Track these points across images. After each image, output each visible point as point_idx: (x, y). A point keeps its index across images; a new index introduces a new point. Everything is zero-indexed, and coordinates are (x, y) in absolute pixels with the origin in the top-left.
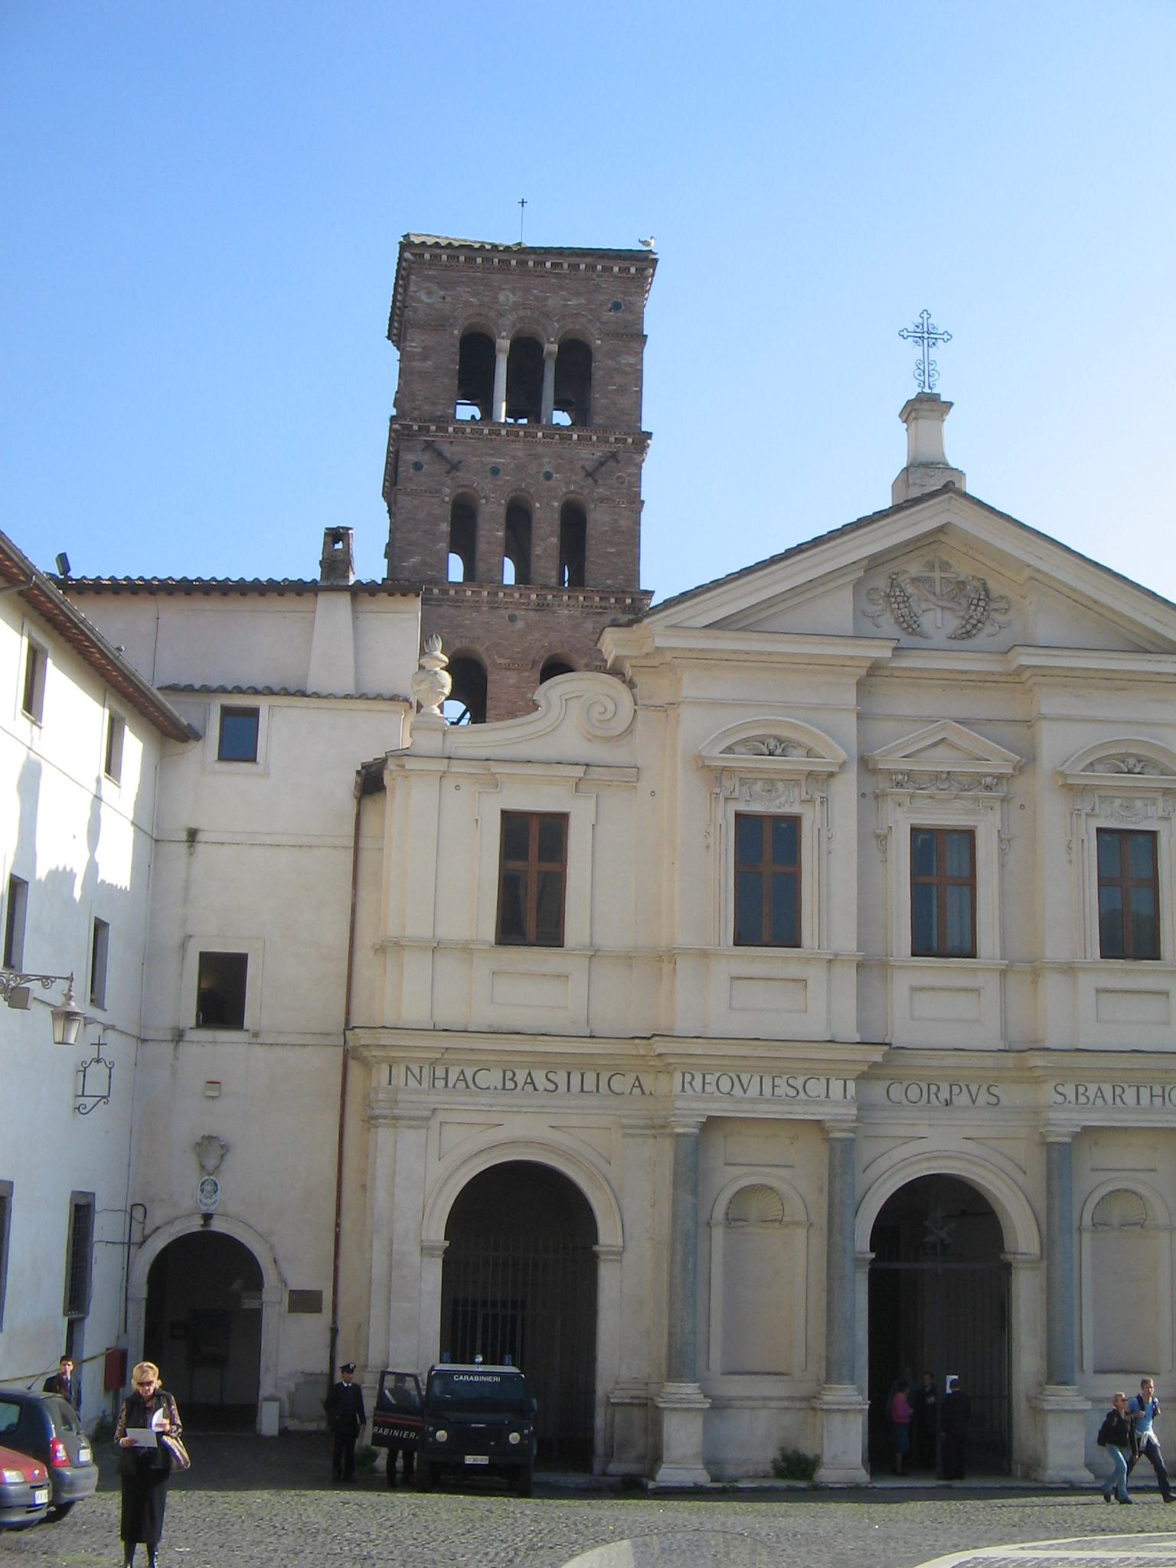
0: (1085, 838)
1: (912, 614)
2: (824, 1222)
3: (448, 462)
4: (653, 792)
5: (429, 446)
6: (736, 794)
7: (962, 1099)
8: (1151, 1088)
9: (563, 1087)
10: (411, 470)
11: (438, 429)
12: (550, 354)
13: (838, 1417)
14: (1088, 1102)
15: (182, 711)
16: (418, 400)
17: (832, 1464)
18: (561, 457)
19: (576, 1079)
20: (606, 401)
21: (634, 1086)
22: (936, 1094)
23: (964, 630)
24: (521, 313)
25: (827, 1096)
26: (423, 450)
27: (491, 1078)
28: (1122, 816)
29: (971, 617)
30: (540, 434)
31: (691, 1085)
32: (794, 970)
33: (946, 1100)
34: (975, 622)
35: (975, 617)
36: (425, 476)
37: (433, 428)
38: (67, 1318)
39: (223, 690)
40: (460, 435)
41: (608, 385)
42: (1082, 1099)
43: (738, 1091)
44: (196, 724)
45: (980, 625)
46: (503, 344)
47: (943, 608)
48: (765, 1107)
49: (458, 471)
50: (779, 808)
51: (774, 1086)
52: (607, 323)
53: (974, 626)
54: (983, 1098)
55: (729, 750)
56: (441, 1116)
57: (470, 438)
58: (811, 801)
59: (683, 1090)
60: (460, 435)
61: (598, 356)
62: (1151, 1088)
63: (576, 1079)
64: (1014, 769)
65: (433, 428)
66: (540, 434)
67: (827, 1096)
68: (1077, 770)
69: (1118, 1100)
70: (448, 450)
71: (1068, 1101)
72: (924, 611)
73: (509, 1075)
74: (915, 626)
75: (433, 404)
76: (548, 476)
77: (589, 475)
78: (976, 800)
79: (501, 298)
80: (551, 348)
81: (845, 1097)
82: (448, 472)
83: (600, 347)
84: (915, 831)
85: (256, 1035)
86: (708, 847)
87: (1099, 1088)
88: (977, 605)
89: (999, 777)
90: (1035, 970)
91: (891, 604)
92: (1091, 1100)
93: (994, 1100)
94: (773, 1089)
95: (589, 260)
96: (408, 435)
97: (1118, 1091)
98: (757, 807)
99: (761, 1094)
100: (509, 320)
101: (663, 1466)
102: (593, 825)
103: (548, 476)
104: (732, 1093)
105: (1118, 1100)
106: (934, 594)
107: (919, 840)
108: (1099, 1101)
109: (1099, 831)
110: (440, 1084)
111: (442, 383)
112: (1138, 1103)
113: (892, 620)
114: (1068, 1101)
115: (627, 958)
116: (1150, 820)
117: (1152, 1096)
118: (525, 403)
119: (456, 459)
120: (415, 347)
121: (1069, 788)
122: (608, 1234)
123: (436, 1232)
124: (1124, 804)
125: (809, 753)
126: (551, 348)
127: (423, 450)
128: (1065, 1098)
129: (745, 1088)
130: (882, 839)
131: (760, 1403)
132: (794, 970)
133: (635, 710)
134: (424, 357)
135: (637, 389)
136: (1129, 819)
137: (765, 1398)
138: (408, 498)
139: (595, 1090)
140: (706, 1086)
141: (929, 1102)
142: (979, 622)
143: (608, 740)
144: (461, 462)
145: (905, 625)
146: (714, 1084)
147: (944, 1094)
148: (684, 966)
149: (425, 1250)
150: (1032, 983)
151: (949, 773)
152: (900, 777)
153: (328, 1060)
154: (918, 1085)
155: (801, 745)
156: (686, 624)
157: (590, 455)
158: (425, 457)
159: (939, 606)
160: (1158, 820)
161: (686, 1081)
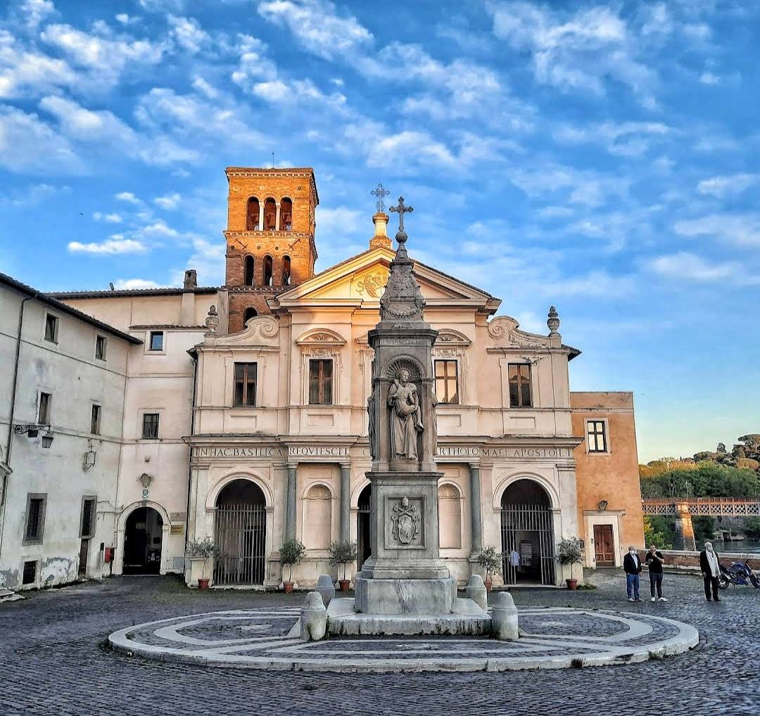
2: (338, 496)
9: (254, 454)
15: (133, 334)
18: (282, 242)
19: (259, 451)
27: (230, 452)
32: (328, 412)
38: (81, 539)
39: (152, 327)
43: (309, 453)
44: (143, 340)
46: (262, 205)
56: (212, 465)
58: (335, 355)
63: (259, 451)
73: (236, 450)
76: (277, 248)
77: (291, 247)
79: (261, 188)
80: (278, 204)
85: (161, 440)
95: (289, 173)
97: (442, 450)
98: (317, 358)
100: (262, 196)
103: (277, 248)
110: (213, 454)
118: (269, 226)
122: (269, 503)
123: (211, 503)
126: (278, 204)
130: (362, 366)
132: (328, 412)
134: (234, 210)
148: (293, 413)
149: (208, 511)
153: (181, 448)
156: (291, 298)
157: (291, 240)
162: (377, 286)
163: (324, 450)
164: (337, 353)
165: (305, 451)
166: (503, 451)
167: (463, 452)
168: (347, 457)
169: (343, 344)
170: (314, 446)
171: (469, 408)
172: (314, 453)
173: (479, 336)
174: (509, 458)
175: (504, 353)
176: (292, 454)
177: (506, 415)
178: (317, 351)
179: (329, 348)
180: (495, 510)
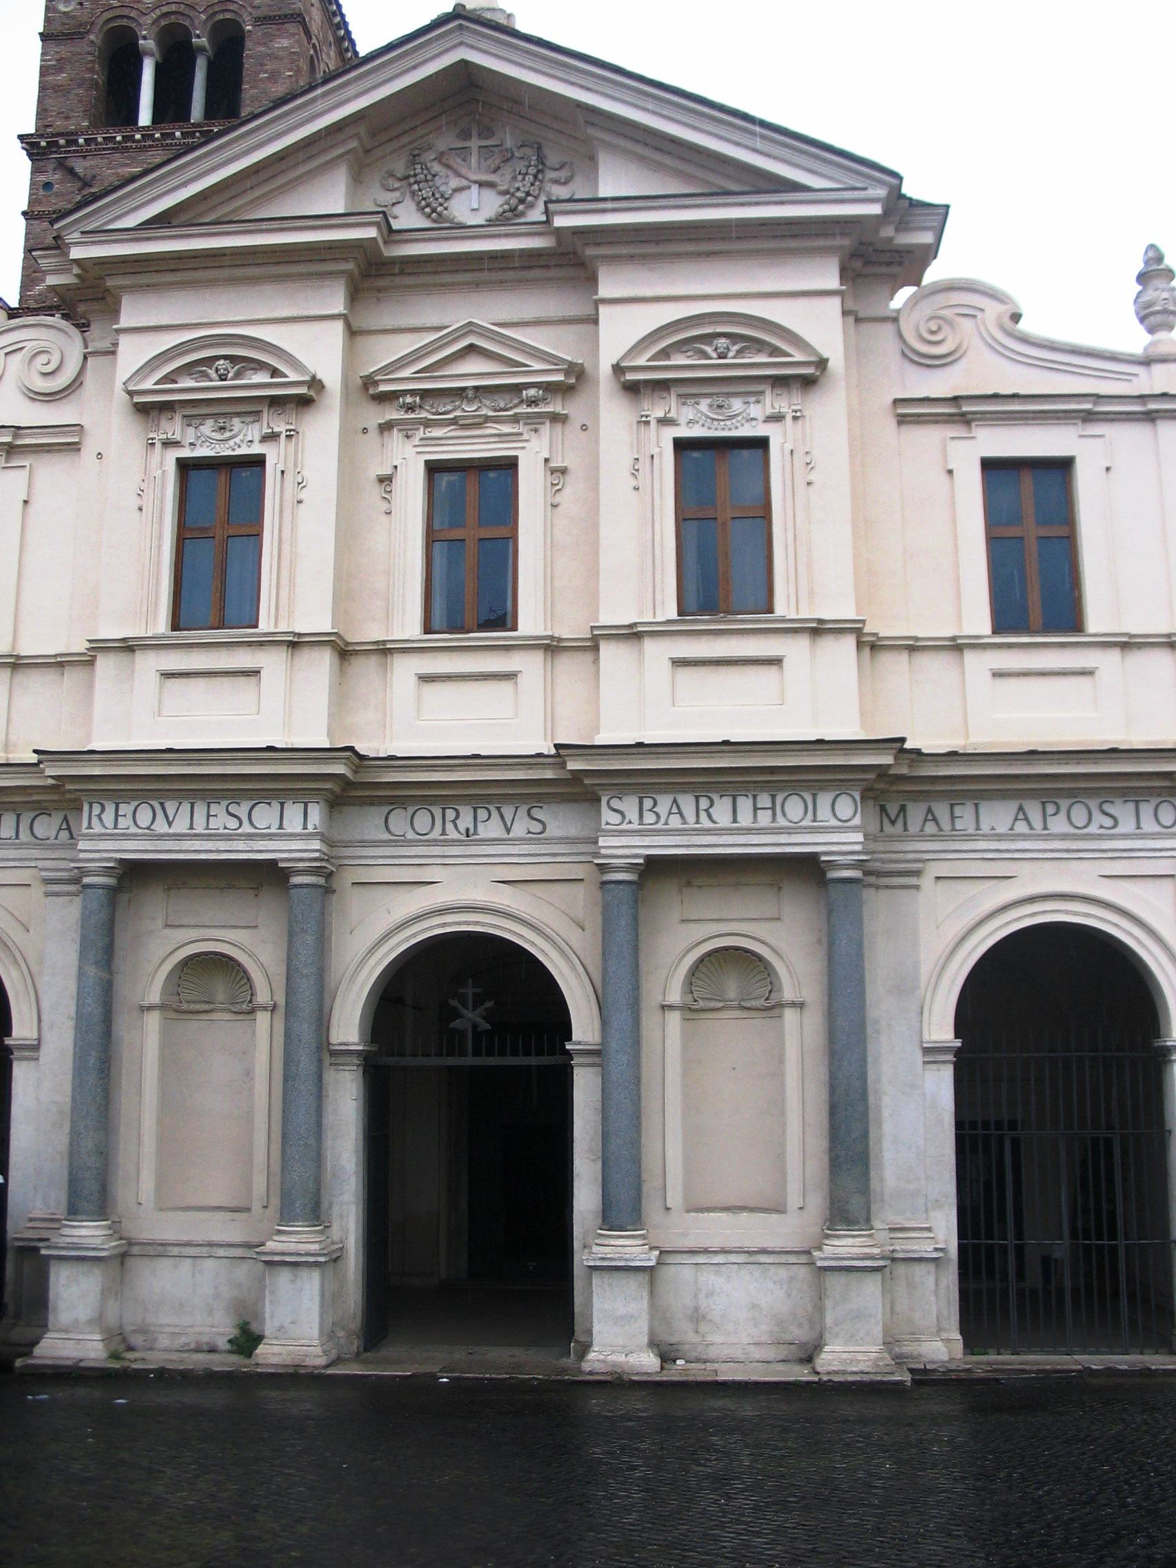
0: (655, 451)
1: (437, 195)
3: (80, 179)
4: (99, 454)
5: (62, 165)
6: (177, 437)
7: (491, 828)
8: (755, 797)
10: (41, 192)
11: (70, 143)
12: (202, 49)
13: (284, 1276)
14: (657, 823)
16: (52, 116)
17: (276, 1338)
20: (256, 91)
21: (60, 829)
22: (454, 822)
23: (506, 207)
24: (165, 9)
25: (281, 827)
26: (54, 170)
28: (713, 419)
29: (518, 189)
30: (178, 134)
31: (101, 819)
33: (468, 830)
34: (519, 194)
35: (521, 189)
36: (56, 196)
37: (62, 142)
40: (93, 147)
41: (257, 73)
42: (649, 818)
43: (161, 827)
45: (530, 198)
47: (481, 184)
48: (197, 845)
49: (91, 186)
50: (234, 450)
51: (209, 816)
52: (259, 7)
53: (522, 201)
54: (519, 830)
55: (169, 378)
57: (104, 149)
58: (272, 437)
59: (90, 827)
60: (93, 147)
61: (249, 44)
62: (755, 797)
64: (567, 373)
65: (62, 142)
66: (178, 134)
67: (281, 827)
68: (642, 361)
69: (703, 815)
70: (80, 166)
71: (627, 820)
72: (456, 190)
74: (440, 209)
75: (67, 118)
78: (515, 419)
81: (305, 828)
82: (80, 190)
83: (250, 31)
84: (434, 469)
86: (140, 509)
87: (675, 801)
88: (527, 174)
89: (549, 388)
90: (592, 645)
91: (410, 185)
92: (663, 820)
93: (537, 827)
94: (208, 819)
96: (38, 154)
97: (704, 803)
99: (191, 828)
100: (148, 20)
101: (48, 1335)
102: (26, 502)
104: (152, 827)
105: (703, 815)
106: (470, 168)
107: (444, 483)
108: (675, 822)
109: (681, 445)
111: (77, 94)
112: (735, 821)
113: (413, 207)
114: (627, 820)
115: (59, 663)
116: (754, 423)
117: (756, 809)
119: (90, 173)
120: (50, 60)
121: (633, 389)
122: (22, 1029)
124: (716, 403)
125: (275, 372)
127: (54, 170)
128: (623, 816)
129: (171, 819)
131: (205, 1251)
133: (85, 358)
135: (291, 73)
136: (722, 423)
137: (211, 1245)
138: (37, 222)
139: (14, 837)
140: (120, 818)
141: (444, 833)
142: (528, 194)
143: (50, 397)
144: (94, 177)
145: (428, 210)
146: (130, 816)
147: (466, 821)
150: (594, 663)
151: (476, 388)
152: (409, 400)
154: (428, 810)
155: (260, 366)
158: (57, 177)
159: (475, 182)
160: (765, 421)
161: (93, 814)
162: (454, 182)
163: (214, 809)
164: (281, 427)
165: (144, 816)
166: (965, 813)
167: (794, 808)
168: (309, 836)
169: (302, 390)
170: (179, 795)
171: (818, 630)
172: (181, 826)
173: (855, 353)
174: (986, 837)
175: (965, 420)
176: (97, 829)
177: (978, 664)
178: (207, 428)
179: (250, 408)
180: (931, 1052)
